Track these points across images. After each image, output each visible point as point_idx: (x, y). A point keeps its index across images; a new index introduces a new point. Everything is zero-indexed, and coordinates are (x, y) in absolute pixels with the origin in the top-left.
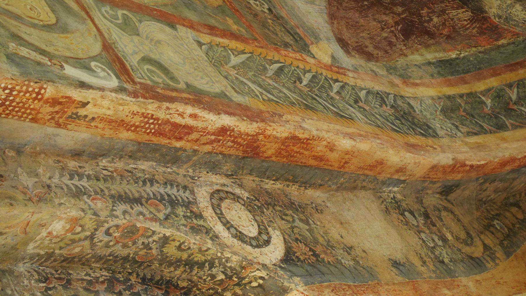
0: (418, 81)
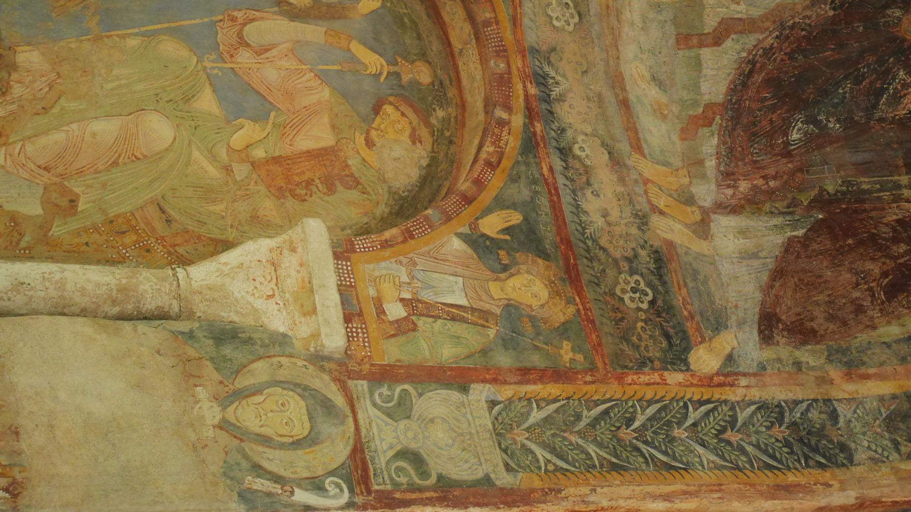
0: (871, 371)
